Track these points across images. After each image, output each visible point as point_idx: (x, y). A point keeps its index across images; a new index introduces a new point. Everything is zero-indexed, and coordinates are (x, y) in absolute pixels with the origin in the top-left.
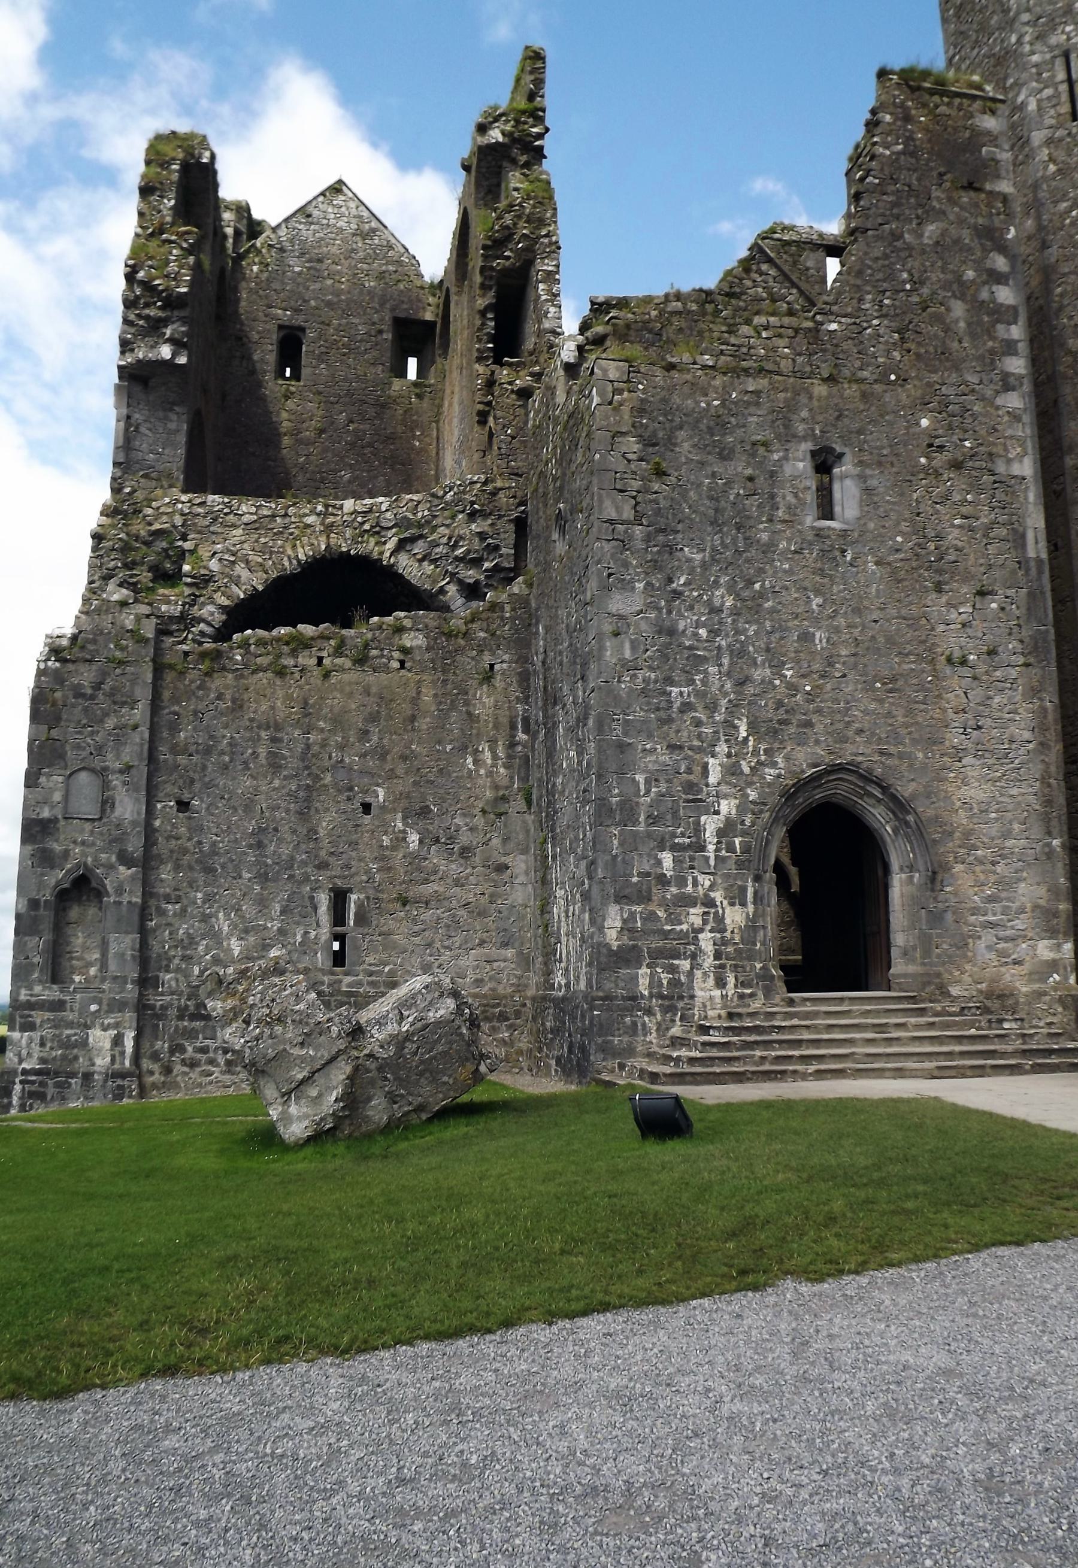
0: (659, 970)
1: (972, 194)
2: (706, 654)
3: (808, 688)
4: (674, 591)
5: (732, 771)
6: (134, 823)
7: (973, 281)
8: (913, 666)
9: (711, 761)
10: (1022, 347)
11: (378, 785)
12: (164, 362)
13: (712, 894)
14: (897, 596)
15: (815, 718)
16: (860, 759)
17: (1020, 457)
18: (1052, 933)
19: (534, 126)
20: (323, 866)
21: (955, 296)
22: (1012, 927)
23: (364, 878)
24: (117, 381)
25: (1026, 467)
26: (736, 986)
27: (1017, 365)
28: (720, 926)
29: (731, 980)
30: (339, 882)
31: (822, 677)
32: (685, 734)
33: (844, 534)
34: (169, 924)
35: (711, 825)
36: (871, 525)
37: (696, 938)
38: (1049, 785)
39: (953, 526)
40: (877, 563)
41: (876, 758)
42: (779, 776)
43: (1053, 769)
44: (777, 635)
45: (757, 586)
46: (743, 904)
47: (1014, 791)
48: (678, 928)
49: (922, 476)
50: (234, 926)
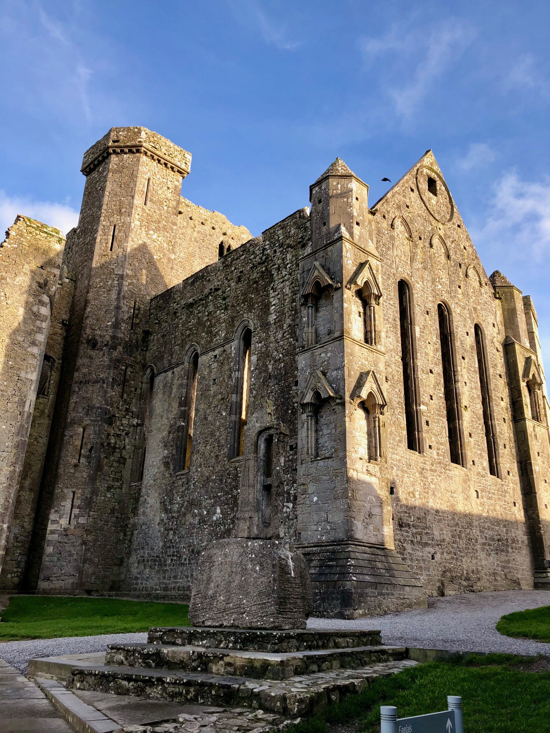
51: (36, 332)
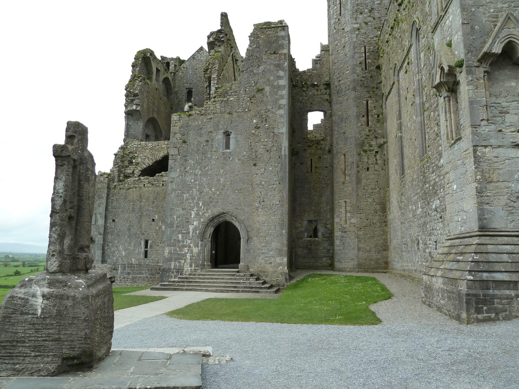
0: (177, 263)
1: (275, 55)
2: (193, 186)
3: (218, 193)
4: (186, 171)
5: (197, 214)
6: (102, 225)
7: (272, 80)
8: (246, 186)
9: (192, 212)
10: (286, 97)
11: (156, 215)
12: (134, 110)
13: (191, 245)
14: (243, 168)
15: (219, 201)
16: (230, 210)
17: (282, 127)
18: (281, 255)
19: (221, 35)
20: (143, 234)
21: (267, 85)
22: (269, 254)
23: (152, 237)
24: (125, 115)
26: (195, 267)
28: (192, 252)
29: (193, 266)
30: (146, 238)
31: (222, 190)
32: (187, 206)
33: (230, 153)
34: (109, 248)
36: (237, 150)
37: (186, 255)
38: (283, 216)
39: (260, 148)
40: (238, 160)
41: (235, 210)
42: (209, 215)
43: (284, 212)
44: (211, 180)
45: (207, 168)
46: (198, 247)
47: (273, 218)
48: (182, 253)
49: (252, 136)
50: (123, 248)
51: (280, 99)
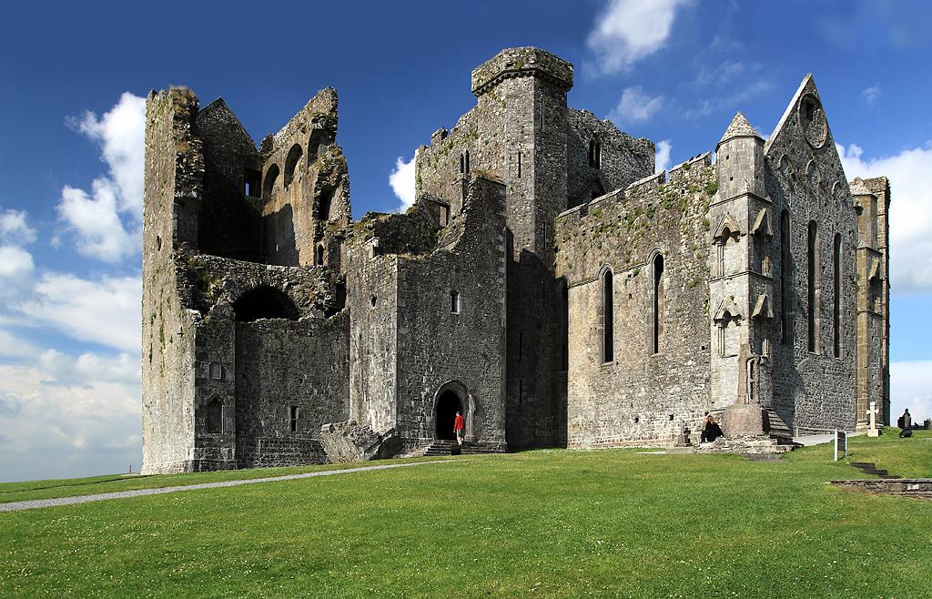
5: (428, 380)
25: (503, 301)
27: (503, 270)
28: (425, 421)
35: (423, 394)
